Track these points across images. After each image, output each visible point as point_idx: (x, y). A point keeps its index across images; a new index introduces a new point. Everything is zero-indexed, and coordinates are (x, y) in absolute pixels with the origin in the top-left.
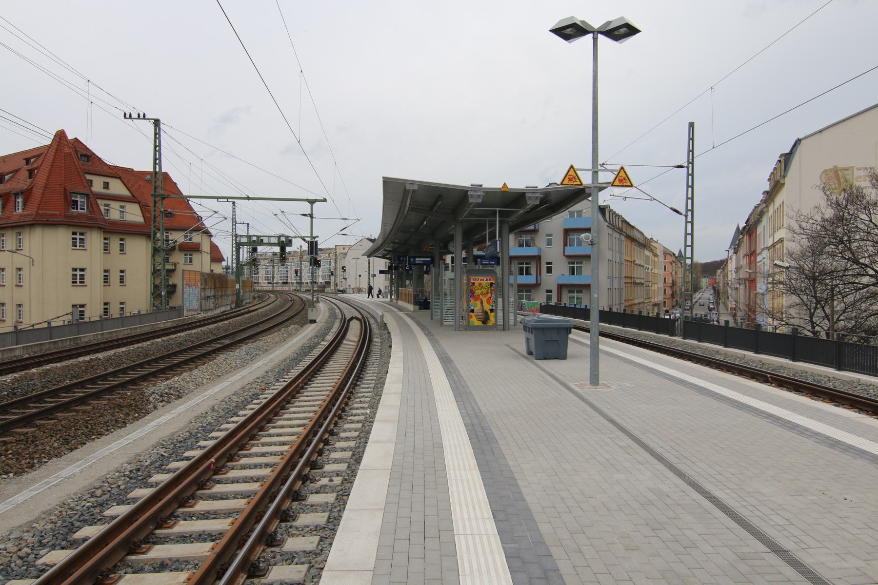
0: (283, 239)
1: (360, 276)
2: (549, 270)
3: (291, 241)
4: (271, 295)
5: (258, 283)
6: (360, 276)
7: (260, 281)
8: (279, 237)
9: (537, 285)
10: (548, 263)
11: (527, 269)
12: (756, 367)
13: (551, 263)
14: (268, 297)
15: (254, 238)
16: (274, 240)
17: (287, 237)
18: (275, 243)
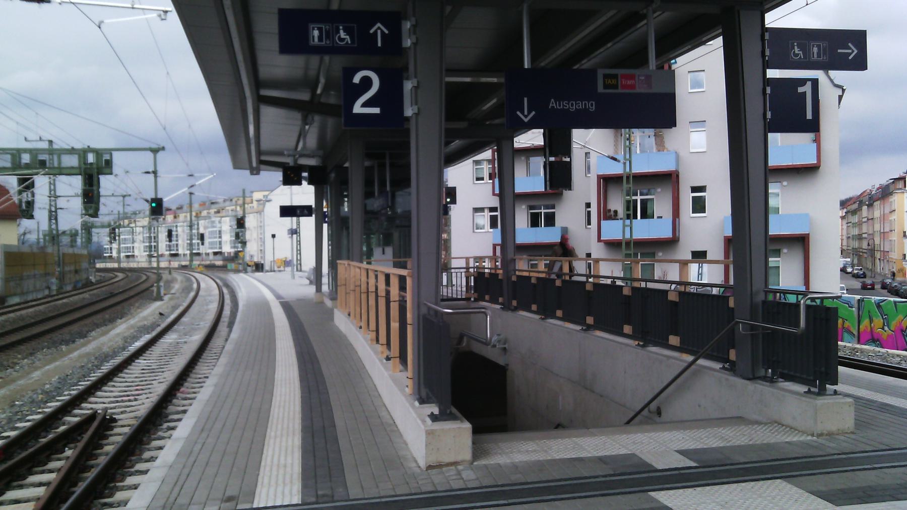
0: (91, 158)
1: (274, 236)
2: (699, 206)
3: (109, 163)
4: (121, 276)
5: (133, 256)
6: (274, 236)
7: (136, 253)
8: (83, 153)
9: (671, 243)
10: (695, 189)
11: (643, 202)
12: (899, 363)
13: (702, 189)
14: (144, 277)
15: (26, 158)
16: (71, 161)
17: (98, 153)
18: (72, 168)
